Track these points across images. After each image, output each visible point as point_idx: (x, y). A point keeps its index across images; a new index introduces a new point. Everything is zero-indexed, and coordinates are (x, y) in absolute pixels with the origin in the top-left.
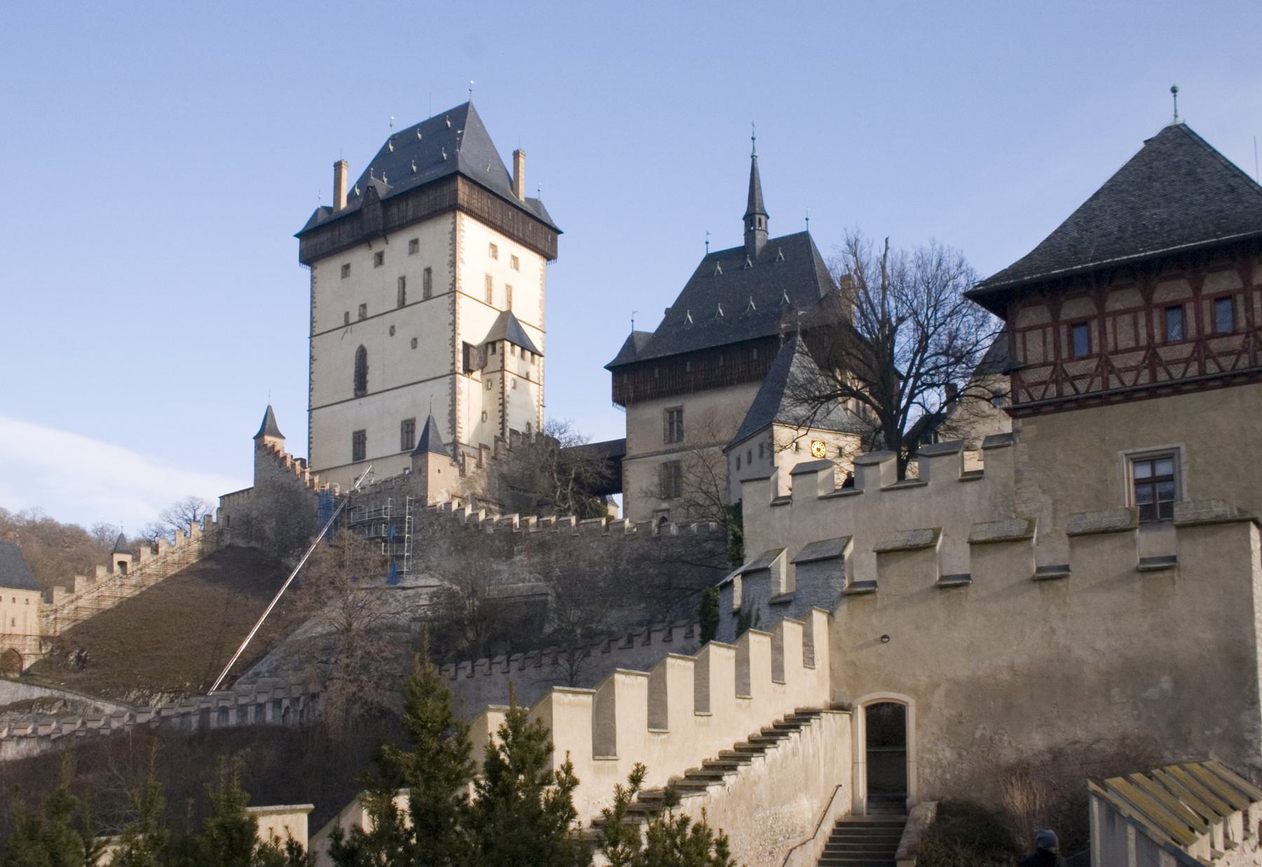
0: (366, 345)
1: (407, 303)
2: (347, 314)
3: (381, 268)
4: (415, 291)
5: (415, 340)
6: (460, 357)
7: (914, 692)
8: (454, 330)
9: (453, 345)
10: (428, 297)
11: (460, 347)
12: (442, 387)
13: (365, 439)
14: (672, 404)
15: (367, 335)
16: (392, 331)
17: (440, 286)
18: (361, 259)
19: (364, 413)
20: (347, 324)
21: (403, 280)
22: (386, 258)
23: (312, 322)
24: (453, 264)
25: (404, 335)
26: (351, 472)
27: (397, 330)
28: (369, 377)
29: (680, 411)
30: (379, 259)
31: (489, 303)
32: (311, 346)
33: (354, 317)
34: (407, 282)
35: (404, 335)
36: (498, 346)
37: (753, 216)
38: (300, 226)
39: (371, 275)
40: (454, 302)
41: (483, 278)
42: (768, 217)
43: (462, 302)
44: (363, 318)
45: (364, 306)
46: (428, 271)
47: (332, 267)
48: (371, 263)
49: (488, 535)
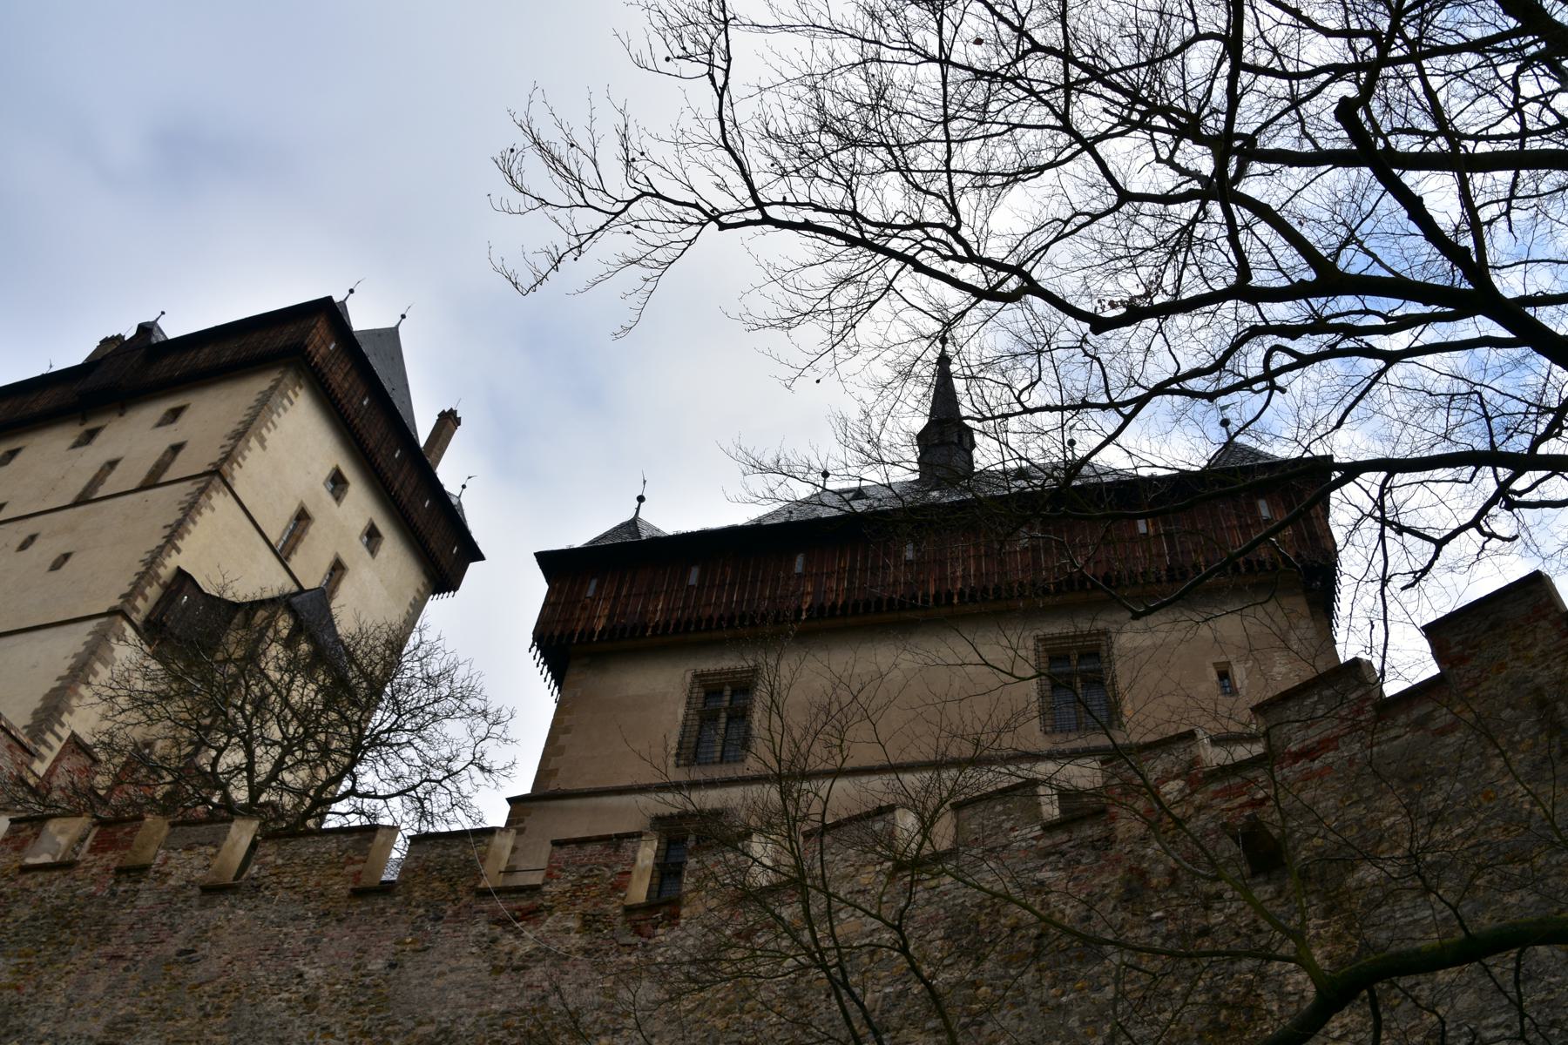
5: (66, 556)
6: (153, 592)
14: (728, 662)
21: (112, 464)
24: (240, 435)
29: (743, 686)
31: (283, 555)
36: (261, 614)
40: (202, 491)
41: (291, 509)
43: (220, 501)
48: (72, 441)
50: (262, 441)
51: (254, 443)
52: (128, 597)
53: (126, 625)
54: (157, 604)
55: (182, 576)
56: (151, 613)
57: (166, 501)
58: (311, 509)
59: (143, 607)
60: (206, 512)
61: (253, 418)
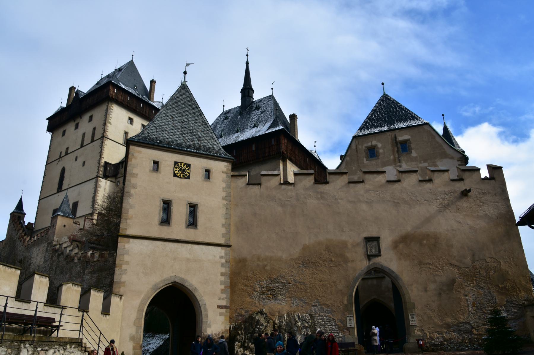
0: (65, 167)
2: (61, 153)
3: (77, 130)
6: (102, 169)
8: (100, 156)
9: (99, 163)
10: (93, 141)
11: (102, 163)
17: (98, 135)
18: (70, 128)
20: (60, 157)
21: (84, 134)
24: (105, 124)
25: (80, 161)
27: (78, 158)
28: (64, 182)
30: (77, 127)
34: (86, 135)
35: (80, 161)
37: (247, 90)
39: (72, 134)
40: (102, 142)
41: (123, 132)
42: (253, 91)
43: (107, 143)
44: (67, 154)
45: (67, 149)
46: (94, 129)
48: (74, 128)
49: (75, 263)
50: (110, 123)
51: (108, 125)
52: (98, 172)
55: (106, 163)
57: (97, 143)
58: (127, 131)
60: (105, 146)
61: (106, 118)
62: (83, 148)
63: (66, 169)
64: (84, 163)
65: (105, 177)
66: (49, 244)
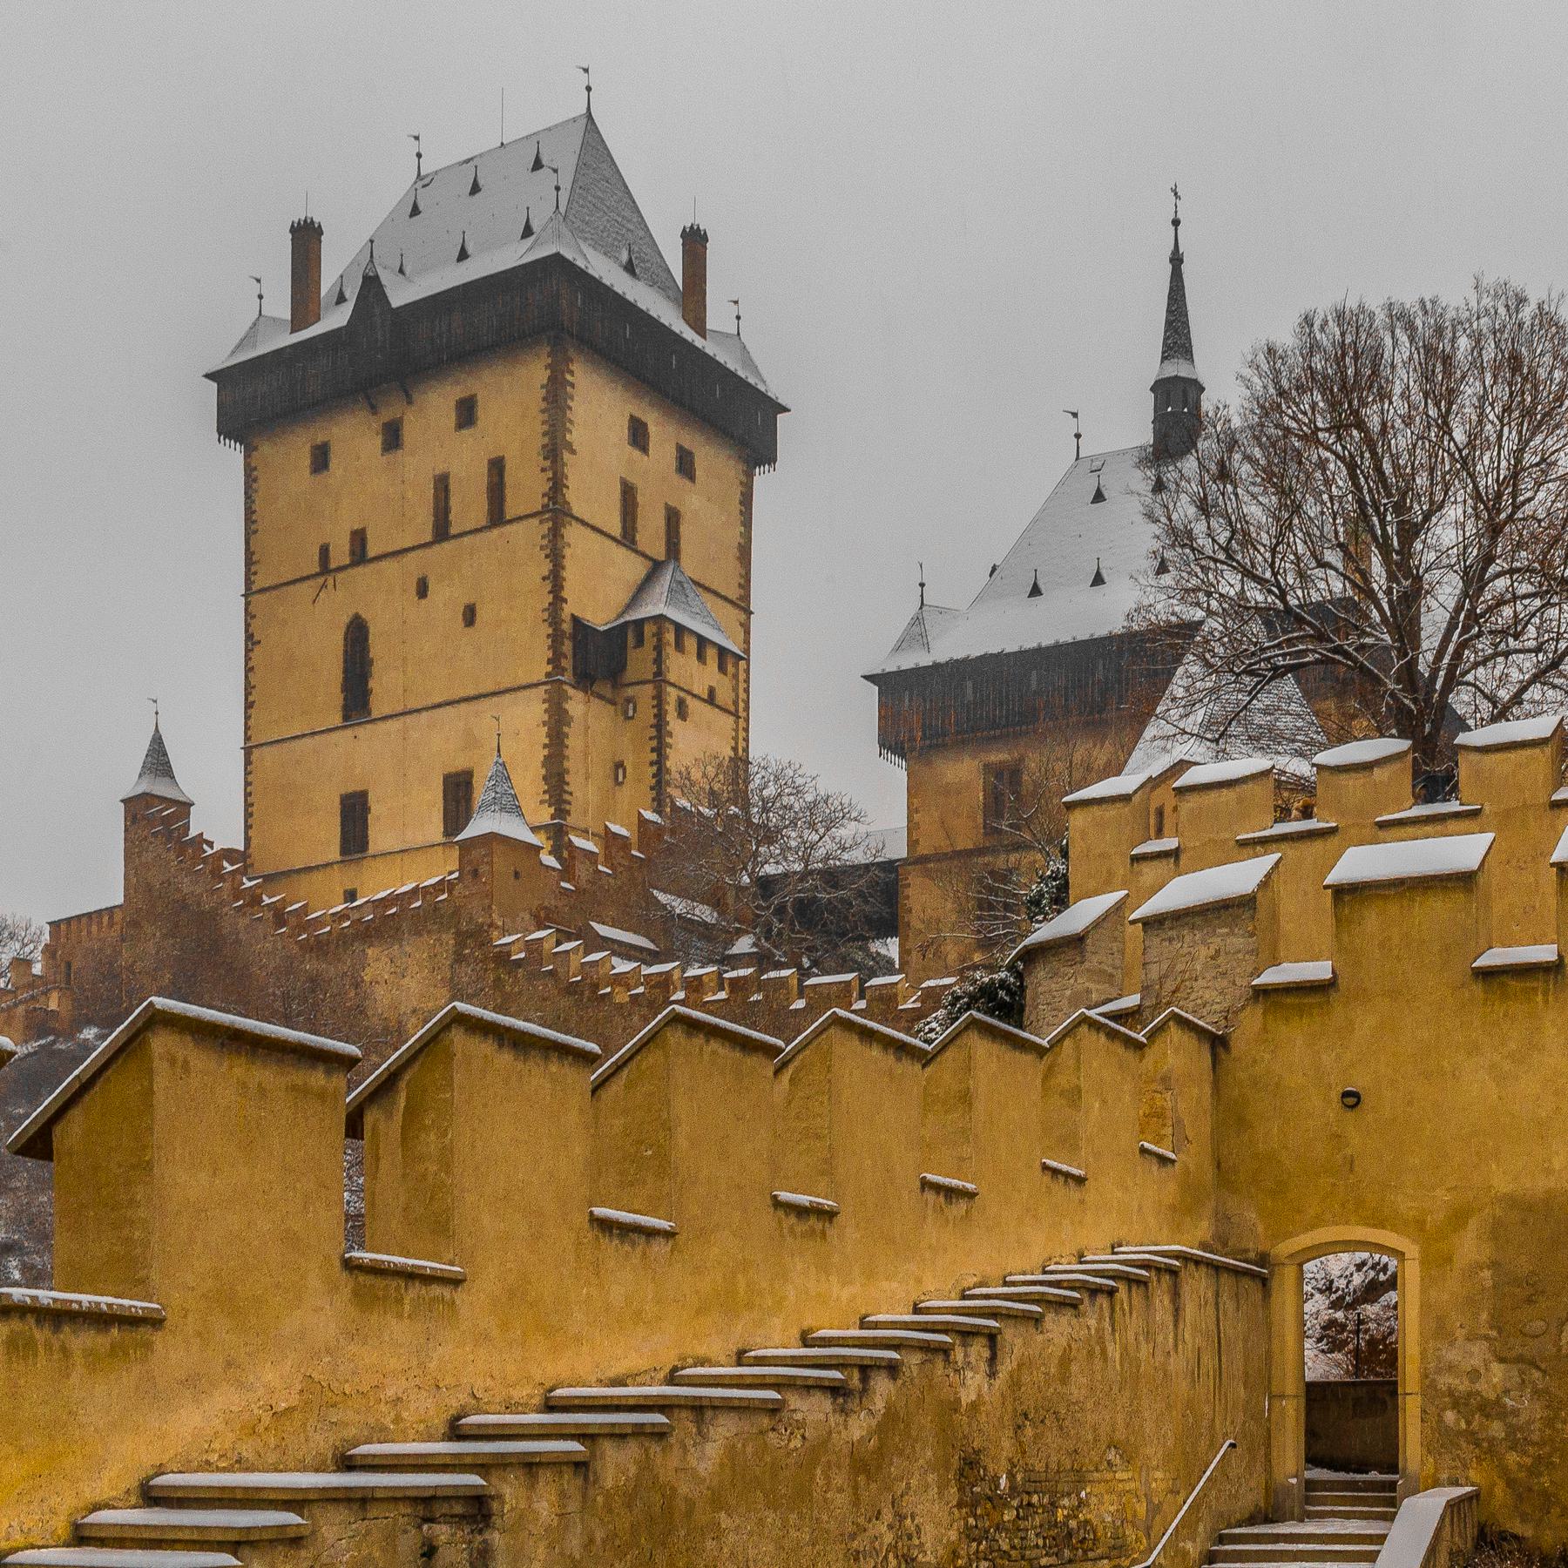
1: (453, 531)
4: (469, 507)
6: (567, 647)
7: (1417, 1228)
11: (567, 627)
12: (529, 713)
13: (366, 809)
15: (377, 595)
16: (422, 590)
18: (353, 437)
19: (362, 756)
21: (442, 484)
22: (410, 433)
23: (250, 561)
26: (339, 880)
27: (432, 586)
30: (392, 438)
32: (248, 614)
33: (340, 555)
35: (446, 597)
38: (221, 359)
47: (294, 449)
48: (378, 441)
52: (555, 661)
53: (566, 687)
54: (575, 655)
55: (576, 620)
56: (575, 668)
59: (567, 663)
62: (446, 546)
63: (373, 630)
64: (470, 616)
65: (585, 680)
66: (462, 938)
